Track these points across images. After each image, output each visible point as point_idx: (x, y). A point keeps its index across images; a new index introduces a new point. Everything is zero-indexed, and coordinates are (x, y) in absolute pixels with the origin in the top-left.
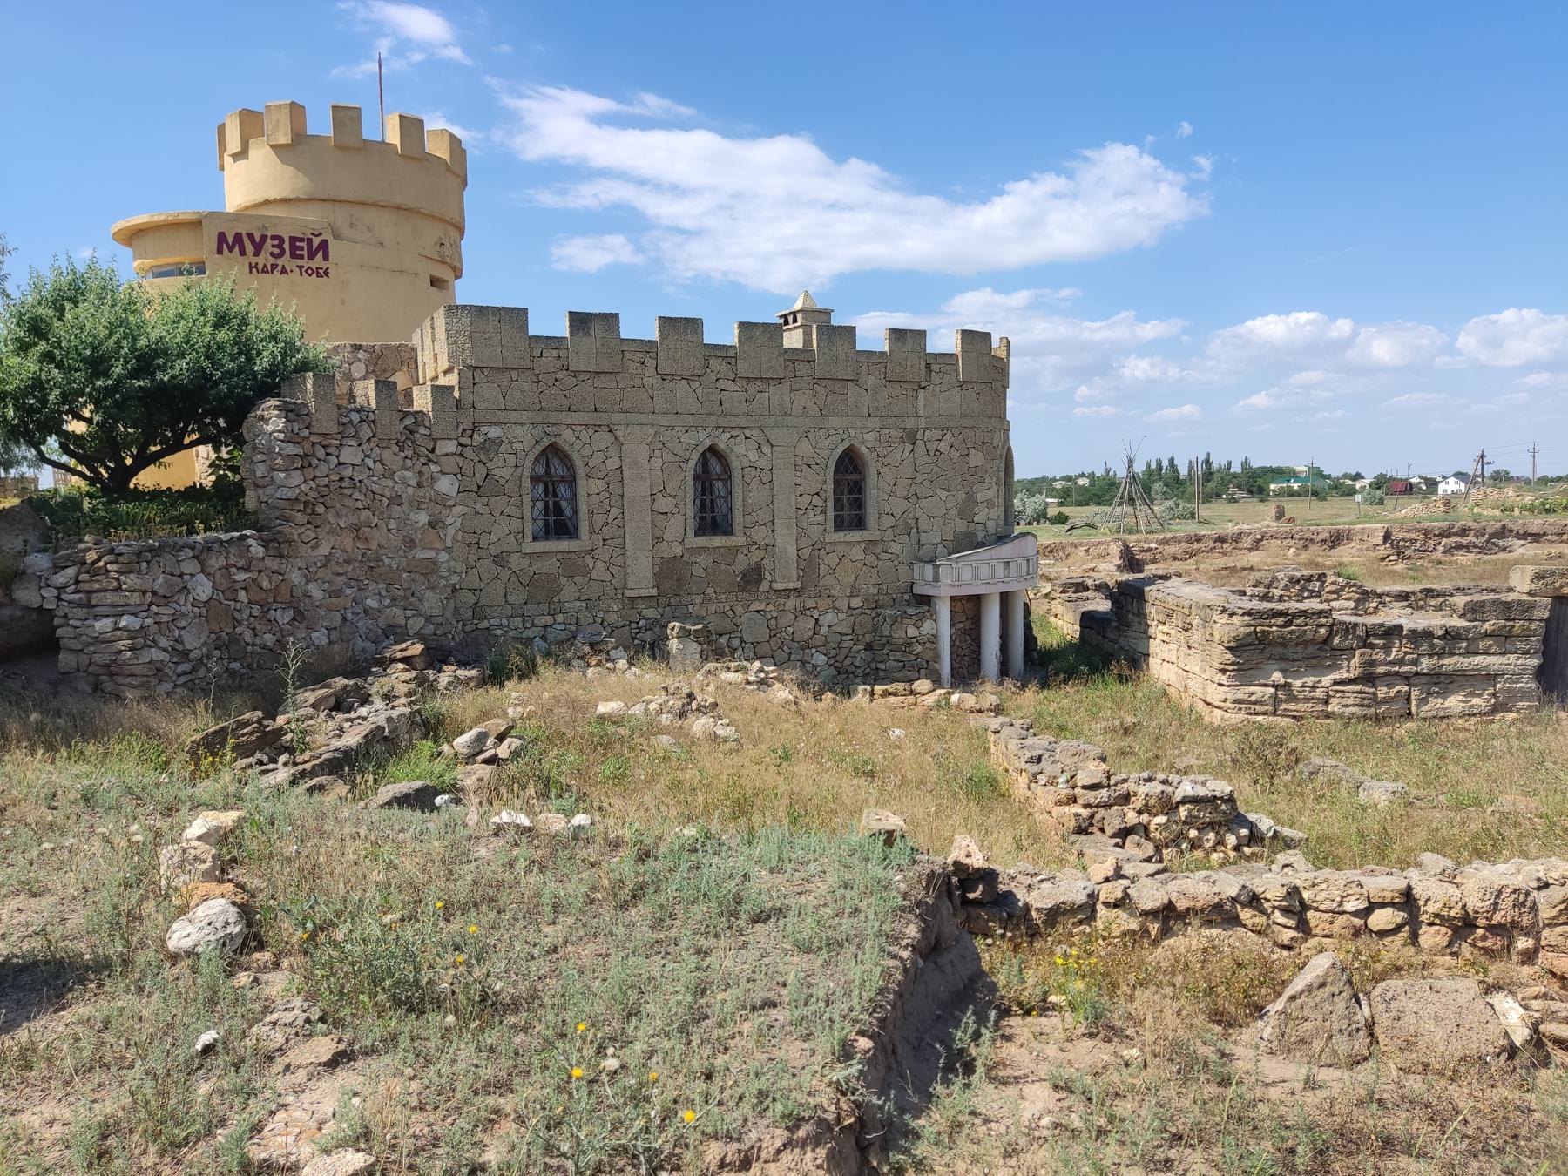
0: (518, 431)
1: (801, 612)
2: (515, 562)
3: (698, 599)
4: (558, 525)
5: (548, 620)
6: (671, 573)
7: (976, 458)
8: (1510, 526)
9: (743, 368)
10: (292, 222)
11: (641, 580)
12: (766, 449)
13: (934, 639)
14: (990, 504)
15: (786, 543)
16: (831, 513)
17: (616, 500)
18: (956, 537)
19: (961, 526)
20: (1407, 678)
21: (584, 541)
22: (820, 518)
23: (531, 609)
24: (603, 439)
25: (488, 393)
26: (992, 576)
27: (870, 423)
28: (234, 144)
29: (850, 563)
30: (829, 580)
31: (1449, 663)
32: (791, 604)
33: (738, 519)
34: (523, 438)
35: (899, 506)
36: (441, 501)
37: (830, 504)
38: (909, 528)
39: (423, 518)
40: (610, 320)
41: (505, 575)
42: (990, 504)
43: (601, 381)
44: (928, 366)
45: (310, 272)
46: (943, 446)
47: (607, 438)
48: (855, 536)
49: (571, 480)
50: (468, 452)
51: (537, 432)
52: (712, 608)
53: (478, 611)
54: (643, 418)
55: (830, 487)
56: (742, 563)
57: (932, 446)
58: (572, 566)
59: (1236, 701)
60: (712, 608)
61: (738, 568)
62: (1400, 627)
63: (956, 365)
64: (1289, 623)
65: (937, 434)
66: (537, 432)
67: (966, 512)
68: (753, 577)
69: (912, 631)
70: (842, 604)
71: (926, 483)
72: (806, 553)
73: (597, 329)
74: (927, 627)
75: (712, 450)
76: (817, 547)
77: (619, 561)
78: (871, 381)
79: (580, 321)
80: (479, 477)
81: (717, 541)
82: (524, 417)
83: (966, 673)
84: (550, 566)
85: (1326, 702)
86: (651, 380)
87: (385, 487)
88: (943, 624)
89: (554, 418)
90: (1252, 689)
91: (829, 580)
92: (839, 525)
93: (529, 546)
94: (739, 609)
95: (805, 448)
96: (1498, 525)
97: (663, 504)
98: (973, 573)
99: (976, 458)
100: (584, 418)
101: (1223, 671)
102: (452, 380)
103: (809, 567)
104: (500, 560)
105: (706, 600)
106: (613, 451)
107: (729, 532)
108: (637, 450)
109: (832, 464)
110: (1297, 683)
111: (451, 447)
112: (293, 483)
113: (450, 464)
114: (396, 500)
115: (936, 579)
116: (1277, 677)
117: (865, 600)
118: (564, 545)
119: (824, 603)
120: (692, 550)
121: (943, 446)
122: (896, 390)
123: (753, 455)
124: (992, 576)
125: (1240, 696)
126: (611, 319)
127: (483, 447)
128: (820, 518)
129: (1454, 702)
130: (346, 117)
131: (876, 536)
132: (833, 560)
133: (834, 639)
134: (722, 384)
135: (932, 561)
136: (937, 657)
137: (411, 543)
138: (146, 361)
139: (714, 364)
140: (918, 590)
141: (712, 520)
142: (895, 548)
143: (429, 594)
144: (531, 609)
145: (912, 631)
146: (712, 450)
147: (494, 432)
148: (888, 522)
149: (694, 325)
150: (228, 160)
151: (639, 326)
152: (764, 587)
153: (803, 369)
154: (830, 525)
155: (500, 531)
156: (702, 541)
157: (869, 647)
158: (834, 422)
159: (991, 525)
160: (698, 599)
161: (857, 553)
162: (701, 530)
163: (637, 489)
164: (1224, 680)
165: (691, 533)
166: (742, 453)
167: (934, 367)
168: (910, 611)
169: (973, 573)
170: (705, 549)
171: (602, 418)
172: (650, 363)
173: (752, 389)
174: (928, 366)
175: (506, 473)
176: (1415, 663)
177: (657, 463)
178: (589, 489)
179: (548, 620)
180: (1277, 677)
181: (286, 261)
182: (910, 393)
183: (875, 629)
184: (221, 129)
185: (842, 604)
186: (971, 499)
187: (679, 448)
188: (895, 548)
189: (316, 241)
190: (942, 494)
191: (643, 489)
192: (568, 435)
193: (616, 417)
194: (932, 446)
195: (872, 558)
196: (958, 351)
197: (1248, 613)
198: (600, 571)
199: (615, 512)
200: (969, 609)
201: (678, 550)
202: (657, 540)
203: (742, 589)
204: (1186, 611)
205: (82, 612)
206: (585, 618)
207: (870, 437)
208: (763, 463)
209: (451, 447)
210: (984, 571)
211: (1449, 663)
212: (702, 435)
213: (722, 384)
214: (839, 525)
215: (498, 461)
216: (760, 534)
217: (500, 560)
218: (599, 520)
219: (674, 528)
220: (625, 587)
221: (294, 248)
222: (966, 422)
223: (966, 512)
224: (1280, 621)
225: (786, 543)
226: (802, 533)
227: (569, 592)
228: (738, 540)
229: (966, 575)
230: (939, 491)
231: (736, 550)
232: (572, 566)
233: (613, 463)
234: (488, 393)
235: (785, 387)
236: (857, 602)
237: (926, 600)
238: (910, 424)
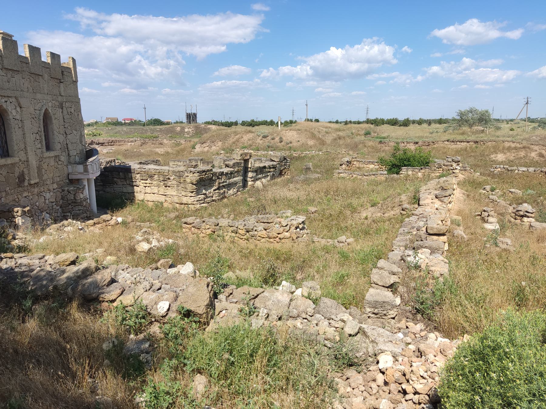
8: (94, 141)
20: (224, 186)
31: (232, 180)
32: (36, 190)
59: (197, 201)
61: (17, 174)
62: (223, 172)
63: (71, 73)
64: (206, 174)
68: (21, 178)
70: (51, 188)
71: (69, 128)
85: (212, 197)
90: (199, 196)
94: (19, 196)
96: (91, 141)
101: (192, 192)
110: (207, 192)
115: (86, 170)
116: (204, 191)
125: (198, 199)
129: (231, 192)
133: (50, 205)
140: (71, 177)
152: (26, 184)
164: (192, 195)
167: (65, 73)
176: (226, 182)
180: (204, 191)
182: (57, 84)
183: (63, 198)
190: (75, 132)
194: (69, 110)
195: (56, 164)
197: (198, 172)
204: (167, 174)
211: (232, 180)
224: (204, 173)
230: (74, 131)
238: (60, 99)
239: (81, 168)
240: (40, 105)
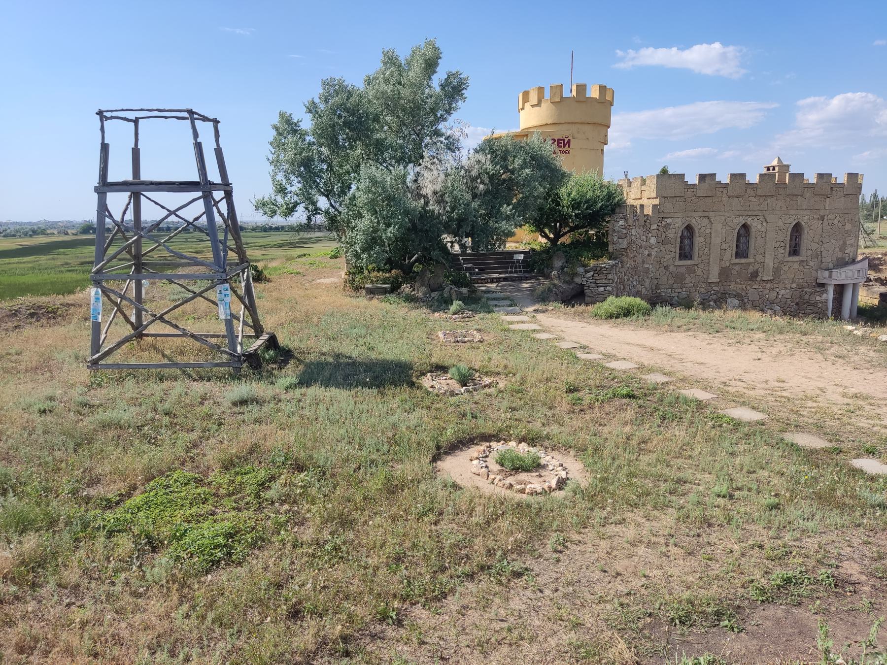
0: (677, 220)
1: (771, 289)
2: (671, 268)
3: (733, 283)
4: (685, 254)
5: (680, 290)
6: (725, 273)
7: (848, 226)
9: (759, 192)
11: (714, 277)
12: (765, 224)
13: (826, 301)
14: (852, 245)
15: (770, 262)
16: (788, 249)
17: (708, 245)
18: (837, 260)
19: (840, 255)
21: (696, 260)
22: (783, 251)
23: (675, 286)
24: (706, 221)
26: (853, 276)
27: (806, 212)
28: (534, 98)
29: (793, 269)
30: (784, 276)
32: (768, 285)
33: (752, 251)
34: (678, 224)
35: (814, 246)
37: (788, 246)
38: (818, 255)
39: (647, 253)
41: (668, 273)
44: (832, 188)
45: (564, 152)
46: (836, 221)
47: (707, 221)
48: (796, 258)
49: (691, 238)
50: (660, 228)
51: (684, 220)
52: (739, 286)
53: (657, 286)
54: (721, 213)
55: (789, 239)
56: (751, 269)
57: (830, 222)
58: (691, 270)
60: (739, 286)
65: (833, 217)
66: (684, 220)
67: (842, 249)
68: (755, 275)
69: (818, 298)
70: (788, 286)
73: (708, 180)
74: (824, 295)
76: (782, 263)
77: (706, 268)
78: (808, 195)
79: (702, 177)
80: (663, 237)
81: (743, 261)
82: (679, 215)
83: (838, 314)
84: (683, 270)
86: (725, 198)
87: (638, 242)
88: (830, 295)
89: (689, 215)
91: (784, 276)
92: (790, 255)
93: (678, 263)
94: (748, 288)
95: (780, 223)
97: (725, 246)
98: (843, 276)
99: (848, 226)
100: (700, 214)
102: (657, 202)
103: (777, 271)
104: (666, 268)
105: (737, 284)
106: (709, 226)
107: (747, 257)
108: (718, 226)
109: (790, 229)
111: (655, 227)
112: (624, 243)
114: (641, 247)
115: (830, 276)
117: (798, 285)
118: (688, 262)
119: (781, 286)
120: (733, 264)
121: (836, 221)
122: (817, 198)
123: (759, 227)
124: (853, 276)
126: (713, 176)
127: (665, 226)
128: (783, 251)
130: (581, 88)
131: (804, 259)
132: (786, 268)
134: (750, 199)
135: (827, 269)
136: (827, 309)
137: (644, 262)
138: (591, 203)
139: (748, 191)
141: (741, 252)
142: (811, 263)
143: (647, 280)
144: (675, 286)
145: (818, 298)
147: (669, 221)
148: (810, 253)
149: (743, 176)
150: (527, 105)
151: (724, 178)
153: (782, 191)
154: (787, 253)
155: (668, 257)
156: (737, 261)
157: (797, 304)
158: (793, 212)
159: (851, 254)
160: (733, 283)
161: (796, 266)
162: (738, 255)
163: (716, 240)
165: (734, 257)
166: (756, 226)
168: (818, 290)
169: (843, 276)
170: (738, 264)
171: (706, 214)
172: (725, 191)
173: (761, 200)
174: (832, 188)
175: (672, 236)
178: (698, 241)
179: (680, 290)
183: (801, 297)
184: (526, 94)
185: (788, 286)
186: (845, 244)
187: (732, 224)
188: (811, 263)
189: (566, 140)
190: (834, 241)
191: (719, 240)
192: (693, 221)
193: (711, 214)
194: (830, 222)
196: (845, 182)
198: (699, 272)
199: (707, 250)
200: (840, 289)
201: (728, 265)
202: (721, 260)
203: (750, 279)
205: (594, 285)
206: (693, 289)
207: (806, 218)
208: (763, 229)
209: (655, 227)
210: (850, 274)
212: (741, 219)
213: (750, 199)
214: (790, 255)
215: (669, 231)
216: (759, 258)
217: (666, 268)
219: (728, 255)
220: (708, 278)
221: (559, 143)
222: (846, 211)
223: (842, 249)
225: (770, 262)
226: (775, 257)
227: (688, 280)
228: (751, 260)
229: (843, 276)
231: (750, 264)
232: (691, 270)
233: (708, 231)
234: (668, 206)
236: (794, 286)
237: (822, 285)
238: (822, 212)
239: (827, 273)
240: (792, 219)
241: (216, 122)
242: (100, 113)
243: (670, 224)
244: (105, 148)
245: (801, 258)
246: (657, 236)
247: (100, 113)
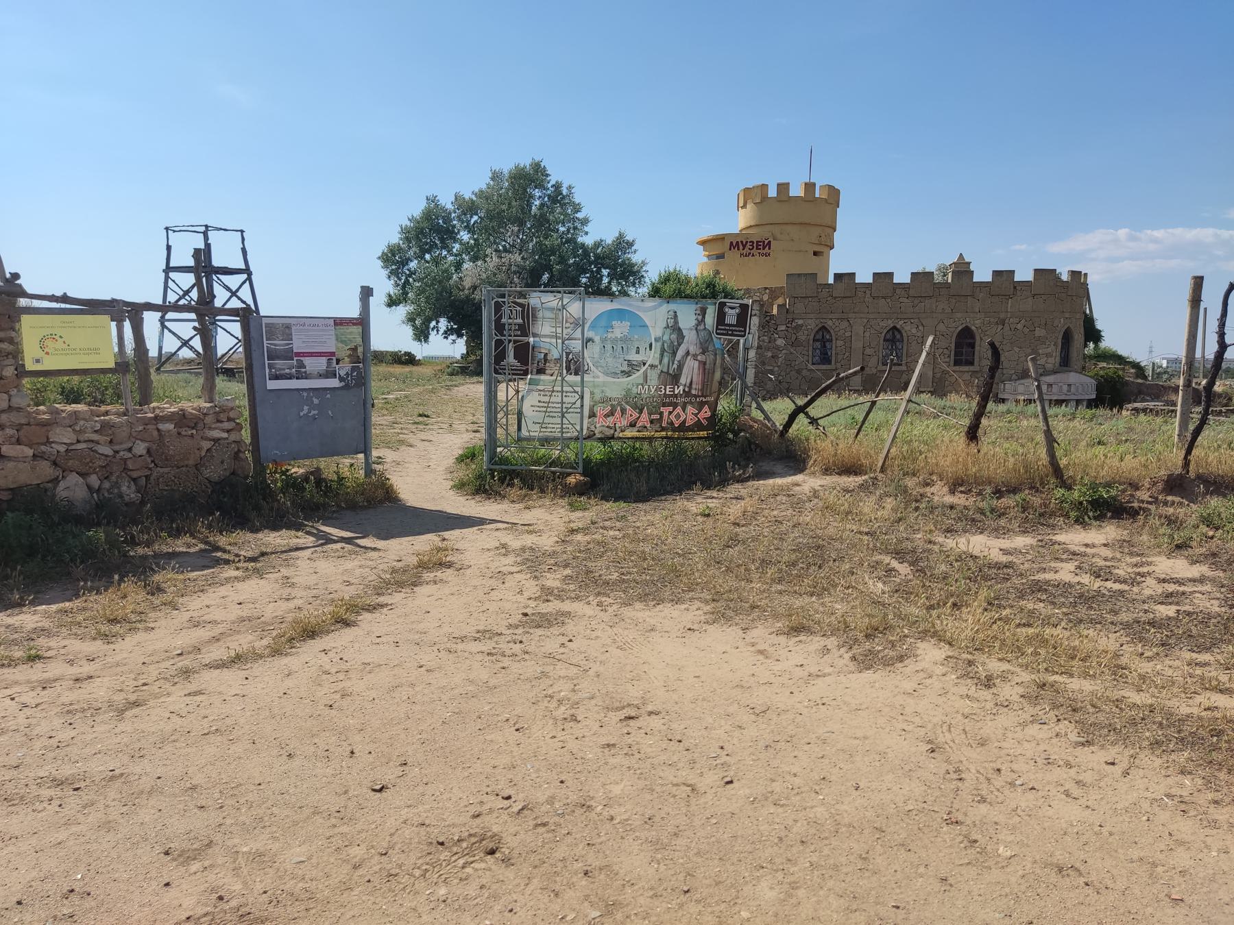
2: (804, 372)
7: (1039, 332)
9: (912, 292)
10: (757, 234)
24: (845, 324)
25: (799, 308)
34: (812, 324)
36: (778, 348)
39: (770, 354)
40: (852, 276)
42: (1048, 355)
43: (845, 300)
46: (1019, 326)
57: (1013, 327)
72: (938, 375)
75: (895, 328)
86: (868, 299)
97: (868, 351)
99: (1039, 332)
100: (837, 316)
104: (799, 372)
111: (783, 328)
113: (782, 334)
121: (1019, 326)
123: (914, 331)
139: (898, 291)
146: (895, 328)
147: (800, 322)
154: (952, 363)
158: (959, 315)
163: (857, 345)
171: (845, 316)
173: (916, 301)
177: (867, 334)
181: (754, 251)
190: (1017, 349)
194: (1013, 327)
201: (874, 371)
217: (799, 372)
218: (840, 357)
231: (903, 372)
233: (848, 334)
235: (934, 300)
238: (1002, 316)
241: (242, 231)
242: (167, 229)
243: (802, 326)
244: (169, 248)
245: (972, 368)
246: (785, 338)
247: (167, 229)
